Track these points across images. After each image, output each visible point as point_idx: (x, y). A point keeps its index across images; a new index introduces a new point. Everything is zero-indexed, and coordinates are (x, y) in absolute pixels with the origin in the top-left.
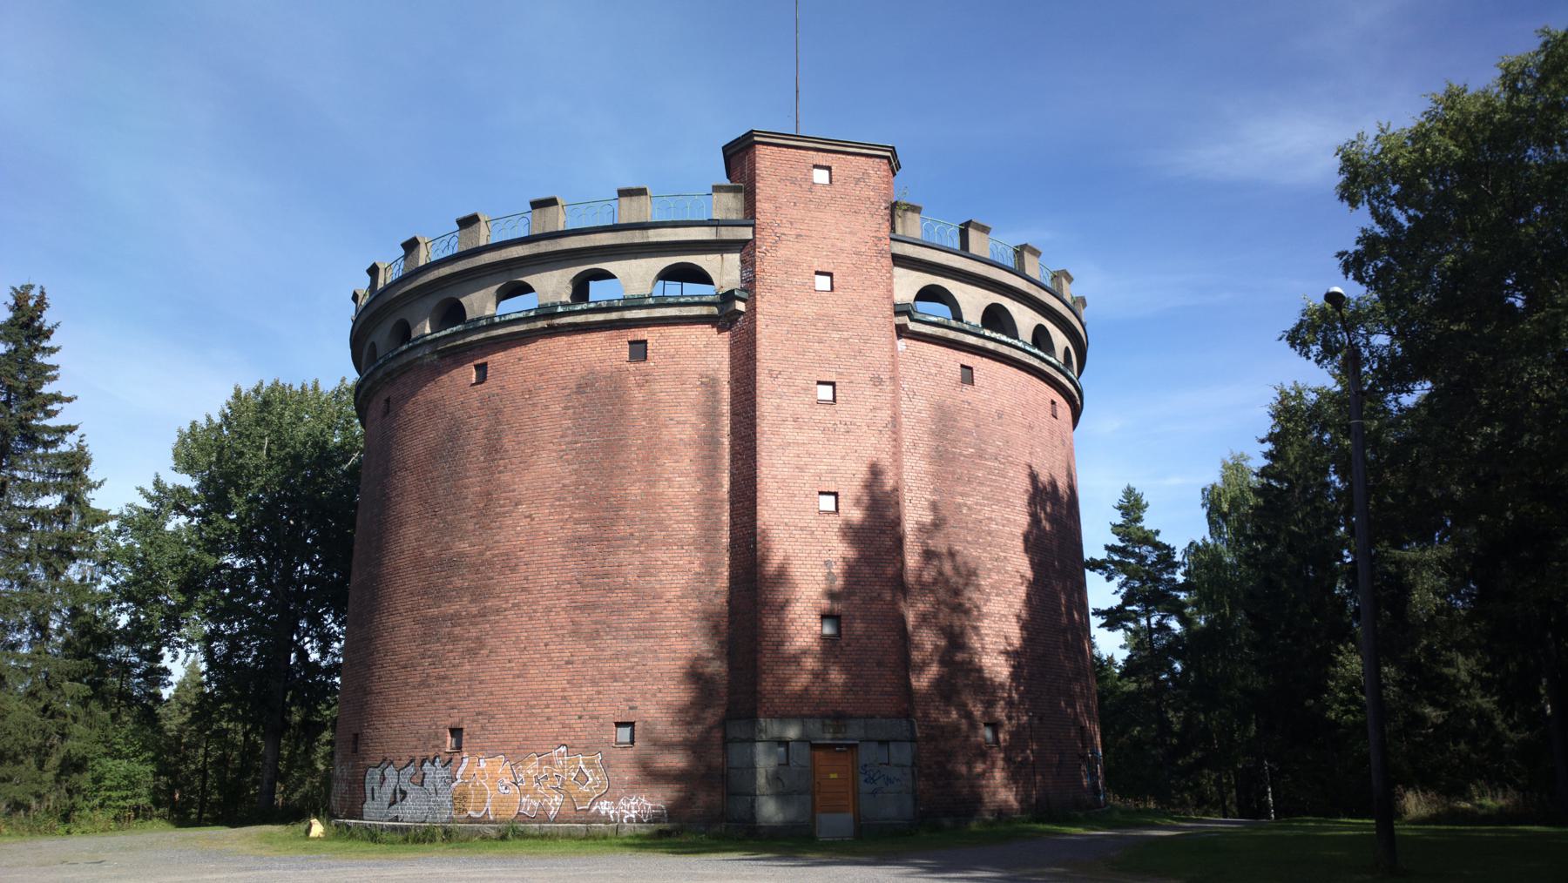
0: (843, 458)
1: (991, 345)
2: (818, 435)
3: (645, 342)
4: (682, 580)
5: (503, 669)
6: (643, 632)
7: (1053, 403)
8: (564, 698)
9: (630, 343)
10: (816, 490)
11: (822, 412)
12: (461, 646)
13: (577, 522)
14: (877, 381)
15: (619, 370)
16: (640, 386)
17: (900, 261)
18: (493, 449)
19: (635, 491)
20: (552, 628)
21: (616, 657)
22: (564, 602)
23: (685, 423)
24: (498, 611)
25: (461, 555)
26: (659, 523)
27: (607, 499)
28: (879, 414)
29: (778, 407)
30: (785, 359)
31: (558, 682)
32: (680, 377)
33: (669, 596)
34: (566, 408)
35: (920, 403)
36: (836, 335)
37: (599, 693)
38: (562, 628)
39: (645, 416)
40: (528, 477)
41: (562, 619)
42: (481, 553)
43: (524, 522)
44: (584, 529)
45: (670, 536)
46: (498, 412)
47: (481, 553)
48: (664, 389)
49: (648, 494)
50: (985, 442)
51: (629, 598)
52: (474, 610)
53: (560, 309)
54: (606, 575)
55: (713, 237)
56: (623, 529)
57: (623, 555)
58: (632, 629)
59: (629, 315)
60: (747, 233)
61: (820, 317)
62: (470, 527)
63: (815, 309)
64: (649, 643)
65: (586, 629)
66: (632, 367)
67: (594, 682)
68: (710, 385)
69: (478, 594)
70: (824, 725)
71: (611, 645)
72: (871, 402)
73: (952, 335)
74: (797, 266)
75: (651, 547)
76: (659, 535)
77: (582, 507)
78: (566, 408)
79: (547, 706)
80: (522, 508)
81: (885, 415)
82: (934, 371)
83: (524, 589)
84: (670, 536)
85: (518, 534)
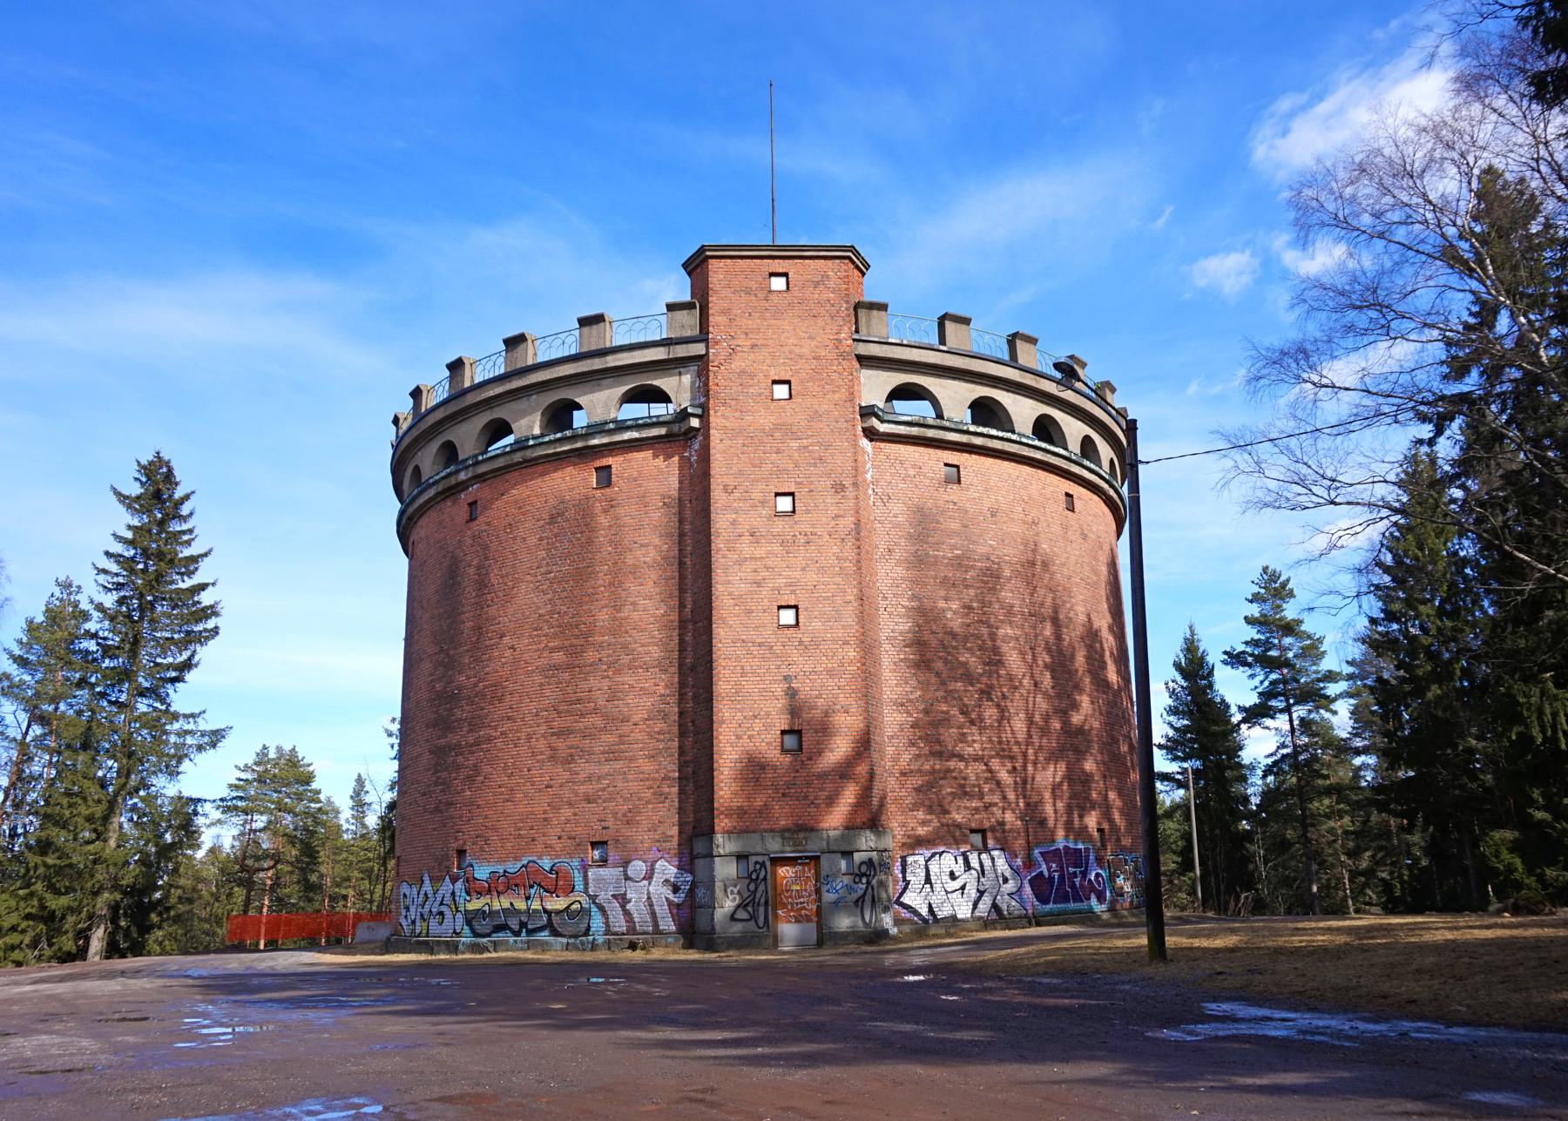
0: (803, 569)
1: (978, 441)
2: (776, 548)
4: (648, 702)
6: (613, 754)
7: (1067, 495)
10: (775, 605)
11: (780, 525)
13: (552, 650)
14: (839, 488)
16: (605, 511)
17: (865, 361)
18: (482, 584)
19: (603, 617)
24: (489, 740)
26: (625, 646)
27: (577, 626)
28: (842, 522)
29: (734, 523)
33: (636, 718)
34: (541, 539)
35: (897, 507)
36: (795, 444)
39: (611, 541)
41: (541, 745)
43: (508, 653)
44: (559, 657)
46: (486, 548)
47: (476, 685)
48: (628, 512)
49: (614, 619)
50: (974, 542)
51: (598, 721)
54: (579, 701)
56: (591, 656)
57: (593, 682)
60: (699, 349)
61: (777, 427)
63: (772, 419)
64: (618, 765)
65: (562, 754)
66: (598, 493)
67: (570, 804)
71: (584, 768)
72: (833, 510)
73: (931, 433)
75: (618, 672)
76: (626, 659)
77: (555, 636)
80: (506, 640)
81: (849, 521)
82: (912, 472)
83: (509, 718)
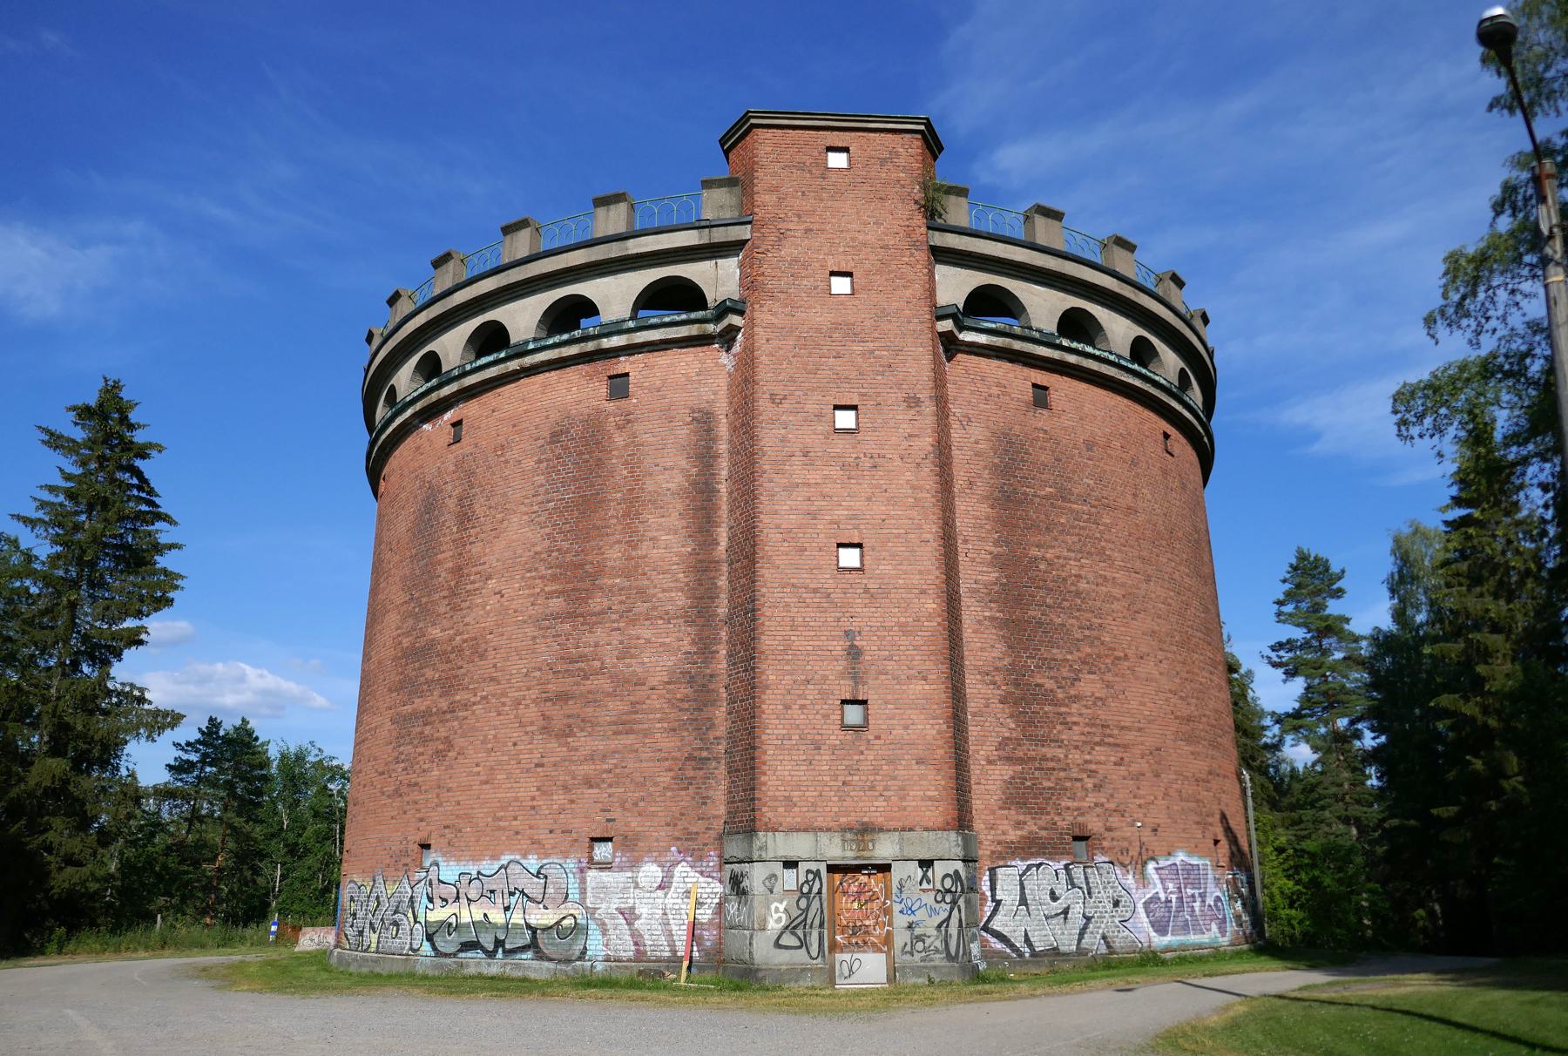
0: (869, 499)
1: (1072, 359)
2: (835, 472)
3: (627, 375)
4: (669, 661)
5: (470, 774)
6: (624, 726)
7: (1166, 436)
8: (533, 808)
9: (610, 377)
10: (834, 542)
11: (840, 444)
12: (431, 748)
13: (549, 596)
14: (913, 402)
15: (599, 411)
16: (619, 427)
17: (942, 255)
18: (465, 518)
19: (614, 555)
20: (522, 725)
21: (591, 758)
22: (534, 693)
23: (672, 468)
24: (466, 706)
25: (432, 643)
26: (642, 593)
27: (581, 566)
28: (917, 443)
29: (784, 440)
30: (792, 380)
31: (527, 788)
32: (668, 415)
33: (653, 681)
34: (540, 462)
35: (977, 431)
36: (858, 348)
37: (572, 802)
38: (532, 723)
39: (626, 463)
40: (500, 544)
41: (532, 713)
42: (451, 639)
43: (494, 600)
44: (557, 604)
45: (654, 608)
46: (471, 473)
47: (451, 639)
48: (647, 431)
49: (630, 558)
50: (1069, 479)
51: (603, 683)
52: (444, 704)
53: (531, 346)
54: (582, 658)
55: (705, 241)
56: (598, 602)
57: (600, 634)
58: (610, 723)
59: (607, 343)
60: (744, 233)
61: (836, 326)
62: (442, 610)
63: (830, 317)
64: (629, 740)
65: (558, 724)
66: (611, 406)
67: (566, 788)
68: (704, 421)
69: (449, 685)
70: (844, 841)
71: (585, 742)
72: (906, 428)
73: (1018, 345)
74: (805, 266)
75: (633, 622)
76: (641, 607)
77: (554, 578)
78: (540, 462)
79: (515, 819)
80: (492, 583)
81: (926, 442)
82: (995, 390)
83: (492, 679)
84: (654, 608)
85: (488, 613)
